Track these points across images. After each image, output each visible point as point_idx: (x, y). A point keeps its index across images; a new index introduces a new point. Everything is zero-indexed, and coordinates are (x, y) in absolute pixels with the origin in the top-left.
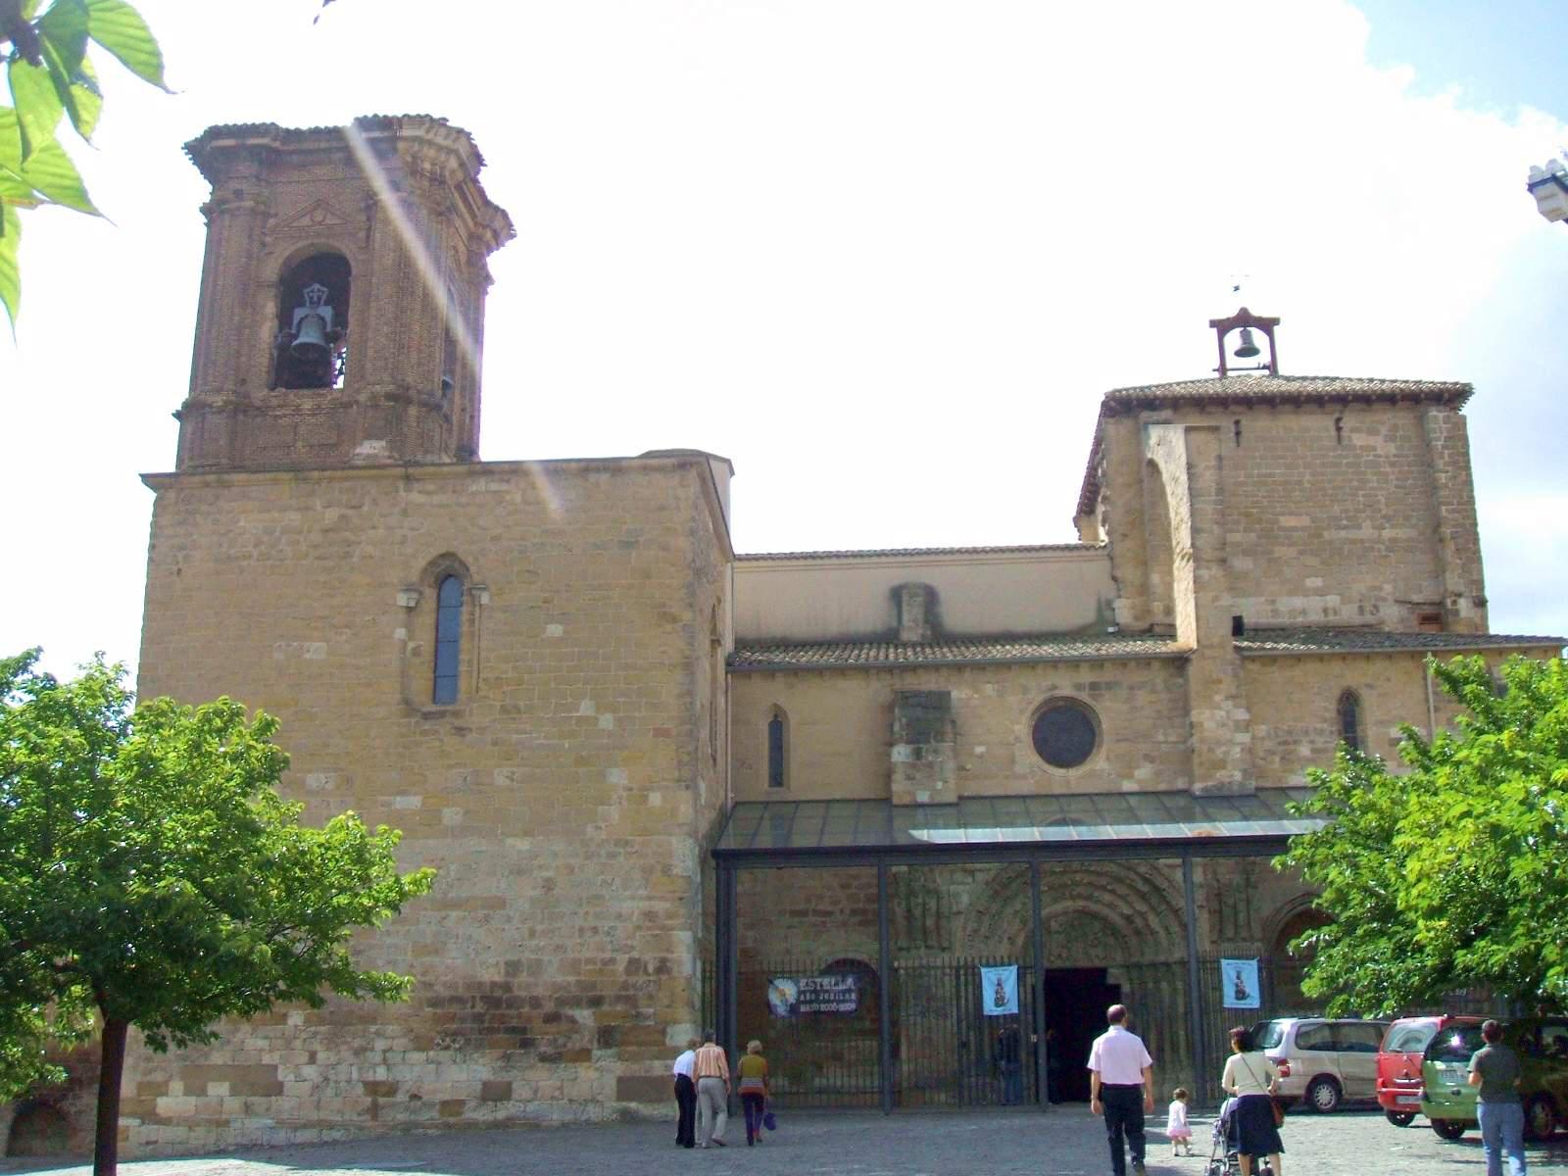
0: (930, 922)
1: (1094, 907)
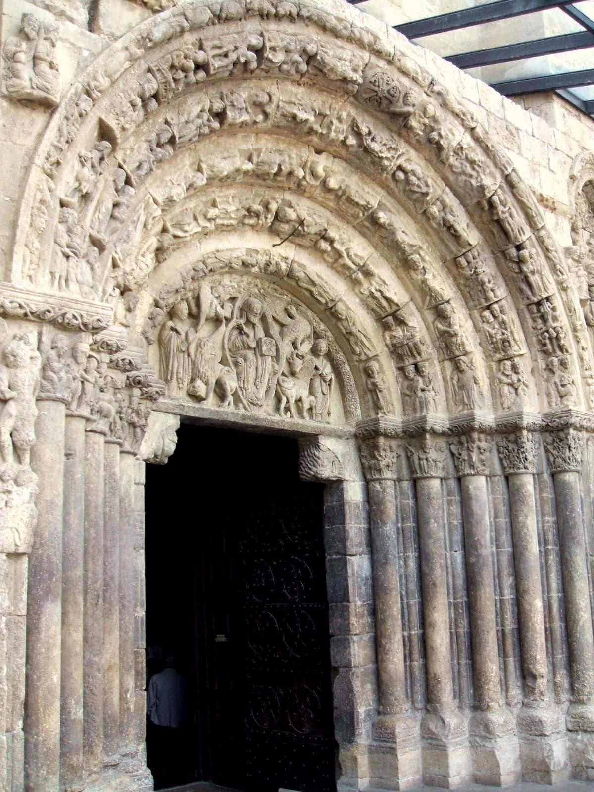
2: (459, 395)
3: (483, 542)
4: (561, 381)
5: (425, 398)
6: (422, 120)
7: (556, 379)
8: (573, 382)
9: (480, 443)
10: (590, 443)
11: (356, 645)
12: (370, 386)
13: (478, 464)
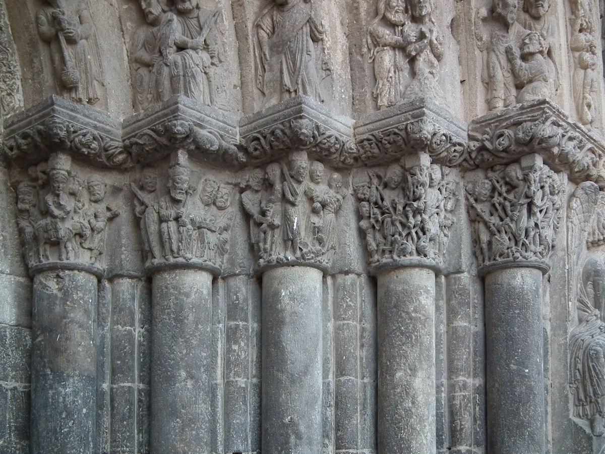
2: (271, 70)
3: (302, 428)
4: (523, 45)
5: (185, 66)
7: (511, 40)
8: (549, 53)
9: (312, 186)
10: (575, 204)
12: (45, 28)
13: (304, 236)
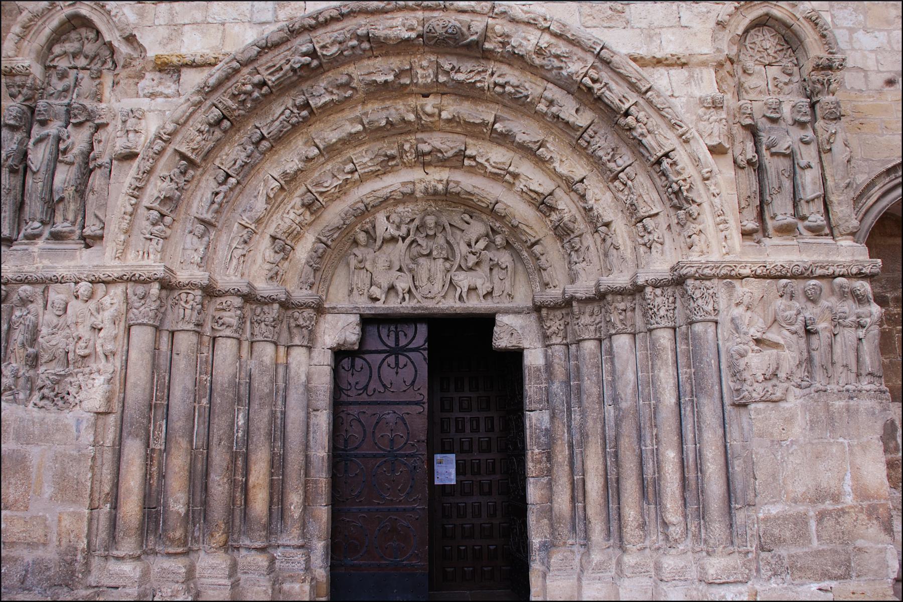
0: (63, 176)
1: (466, 182)
6: (496, 40)
11: (531, 486)
